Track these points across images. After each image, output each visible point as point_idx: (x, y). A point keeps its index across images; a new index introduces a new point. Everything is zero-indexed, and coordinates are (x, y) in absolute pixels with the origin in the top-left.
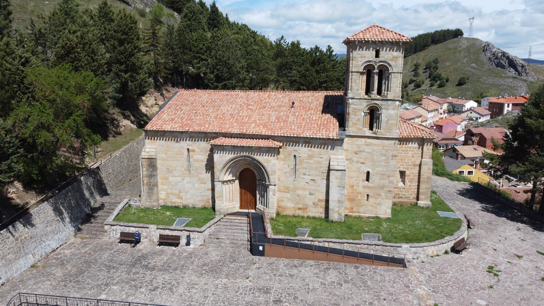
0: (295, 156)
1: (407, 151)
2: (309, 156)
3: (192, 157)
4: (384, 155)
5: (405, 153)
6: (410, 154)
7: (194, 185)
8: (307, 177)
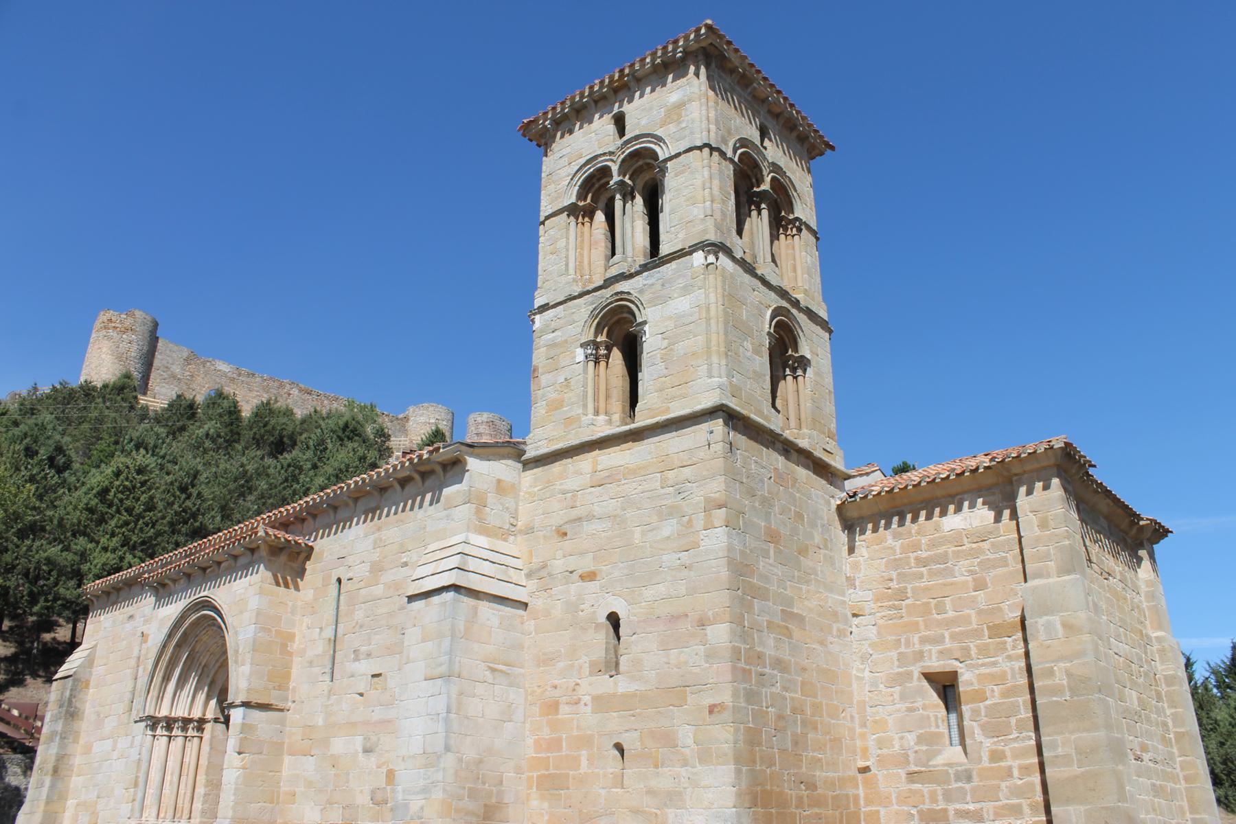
1: (943, 558)
4: (673, 512)
5: (932, 574)
6: (962, 571)
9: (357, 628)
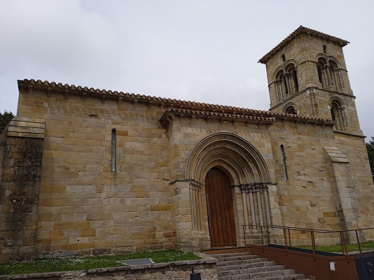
0: (282, 146)
2: (299, 146)
3: (122, 145)
7: (122, 201)
8: (303, 178)
9: (297, 165)
